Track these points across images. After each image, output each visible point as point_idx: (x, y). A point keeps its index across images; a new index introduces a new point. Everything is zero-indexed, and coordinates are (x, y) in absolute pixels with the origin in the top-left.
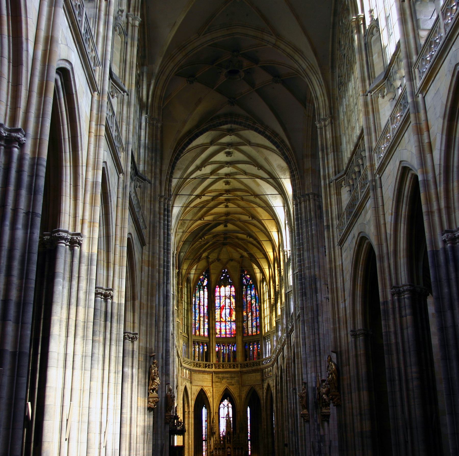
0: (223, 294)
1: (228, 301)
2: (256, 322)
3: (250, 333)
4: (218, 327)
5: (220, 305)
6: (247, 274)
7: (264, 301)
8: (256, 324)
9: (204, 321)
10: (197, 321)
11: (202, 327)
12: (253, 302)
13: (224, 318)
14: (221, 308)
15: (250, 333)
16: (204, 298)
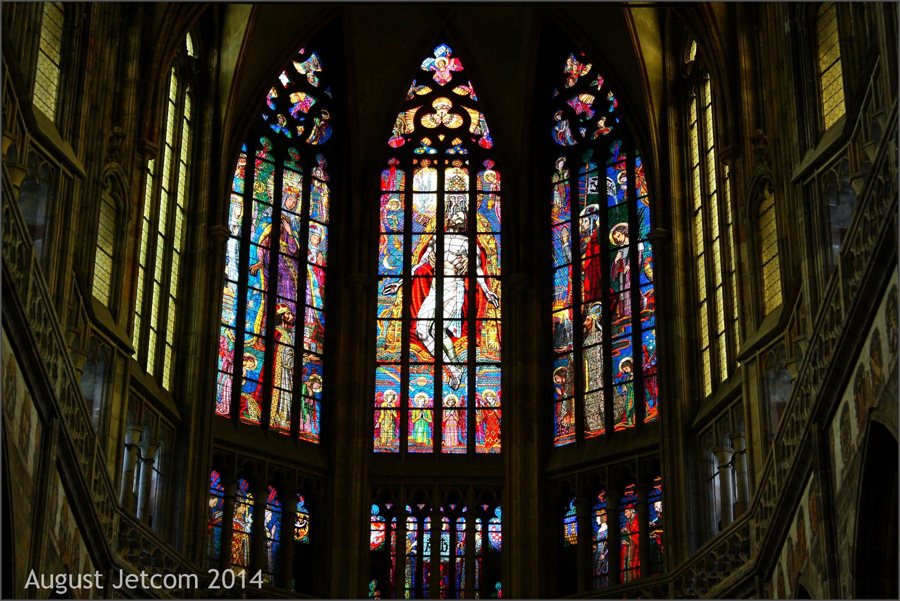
0: (425, 205)
1: (455, 244)
2: (638, 351)
3: (595, 424)
4: (389, 396)
5: (407, 265)
6: (584, 85)
7: (688, 213)
8: (637, 365)
9: (298, 349)
10: (249, 340)
11: (282, 379)
12: (619, 236)
13: (431, 345)
14: (412, 285)
15: (595, 424)
16: (305, 217)
